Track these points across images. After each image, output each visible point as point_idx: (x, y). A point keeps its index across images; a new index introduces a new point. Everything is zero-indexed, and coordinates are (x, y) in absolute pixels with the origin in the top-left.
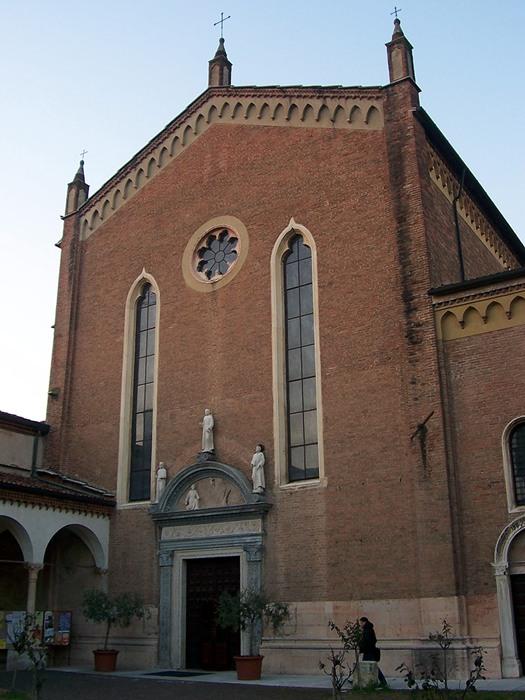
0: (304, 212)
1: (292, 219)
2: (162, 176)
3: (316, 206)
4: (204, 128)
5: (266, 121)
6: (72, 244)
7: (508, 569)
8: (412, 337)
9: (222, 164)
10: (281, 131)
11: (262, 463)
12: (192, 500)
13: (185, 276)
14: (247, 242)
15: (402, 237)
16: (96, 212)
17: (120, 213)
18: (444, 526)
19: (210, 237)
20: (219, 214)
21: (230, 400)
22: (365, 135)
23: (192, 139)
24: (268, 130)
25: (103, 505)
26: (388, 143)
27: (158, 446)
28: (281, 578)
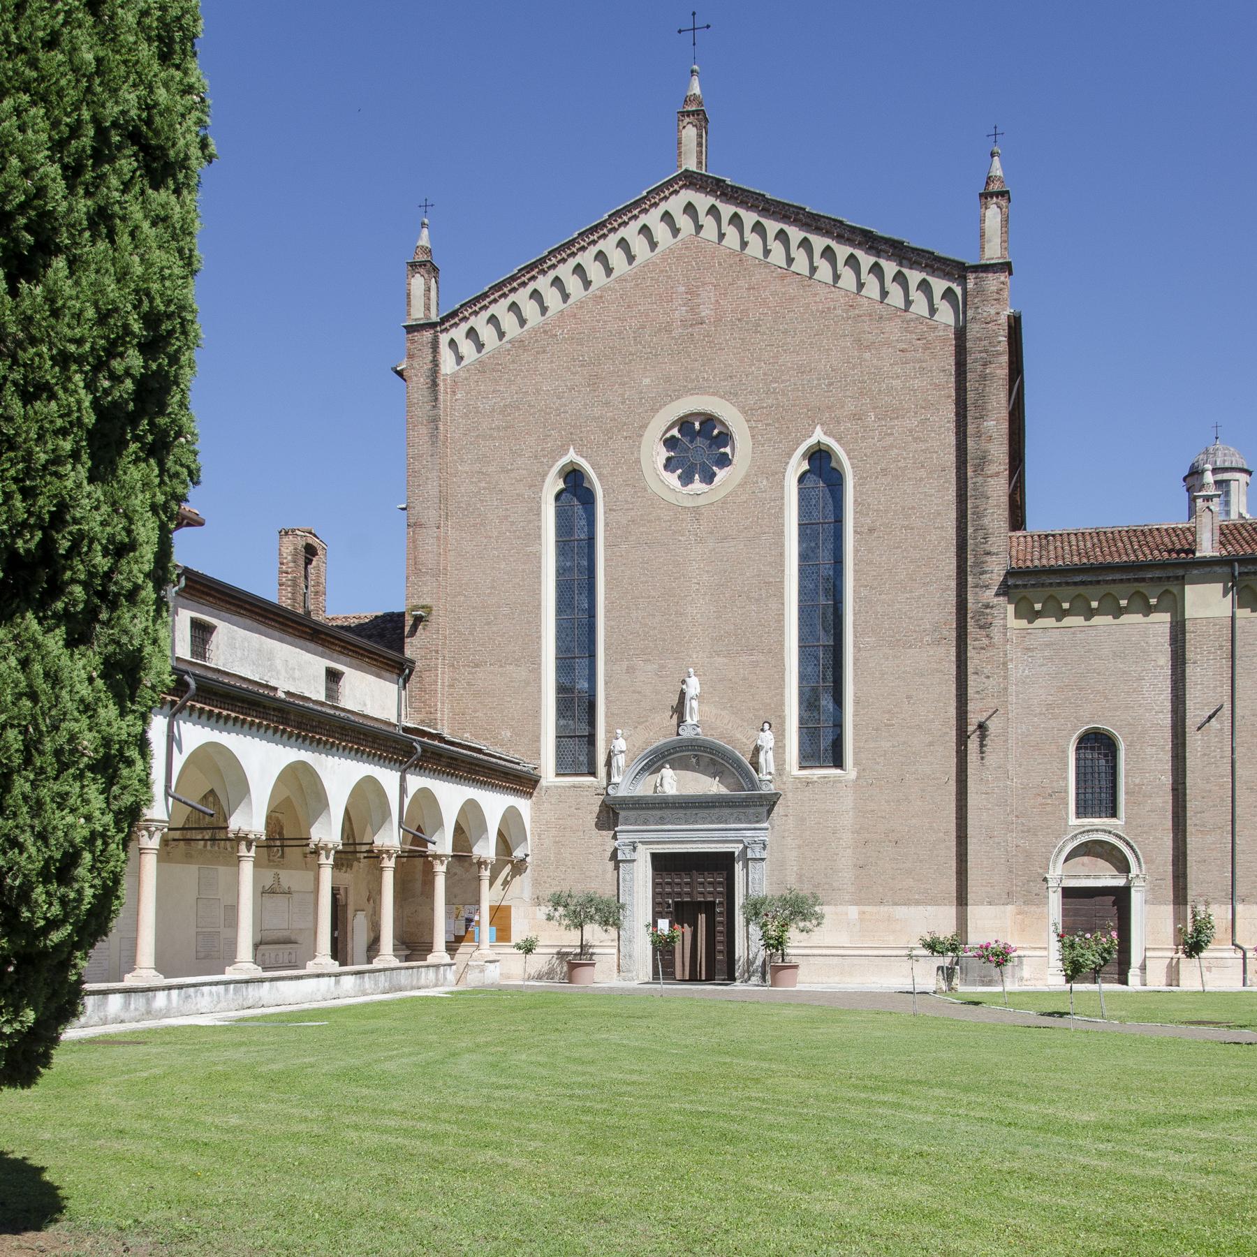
1: (818, 428)
3: (857, 417)
21: (720, 660)
27: (607, 708)
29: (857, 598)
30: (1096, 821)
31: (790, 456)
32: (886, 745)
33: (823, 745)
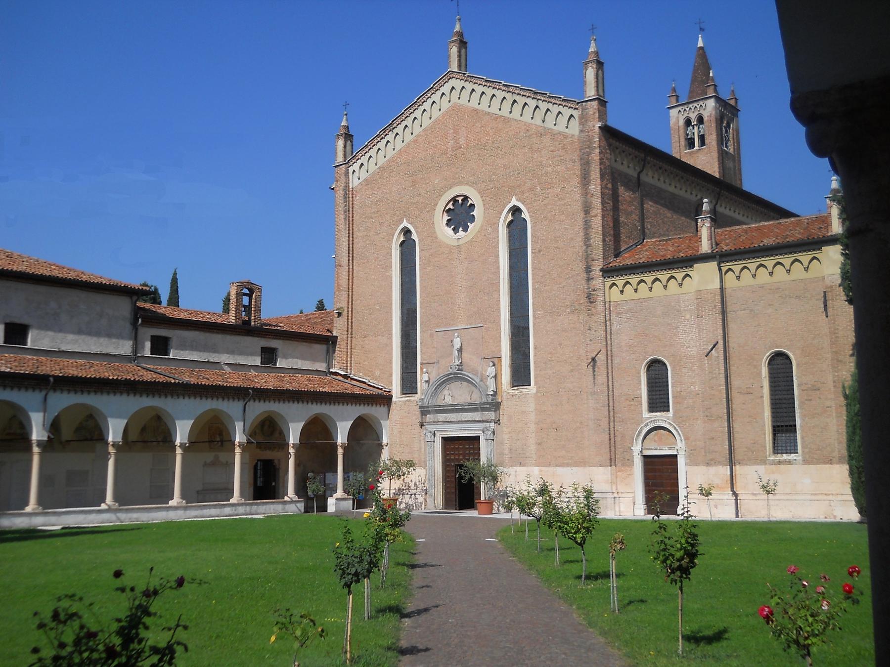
0: (523, 193)
2: (415, 141)
3: (532, 189)
4: (445, 105)
5: (494, 109)
6: (345, 190)
7: (641, 452)
8: (590, 298)
9: (462, 141)
10: (506, 120)
11: (493, 374)
12: (447, 397)
13: (437, 230)
14: (482, 208)
15: (587, 226)
16: (362, 164)
17: (382, 169)
18: (604, 423)
19: (454, 200)
20: (460, 183)
22: (566, 137)
23: (436, 114)
24: (497, 118)
25: (385, 400)
26: (581, 150)
28: (507, 452)
29: (534, 289)
30: (658, 414)
31: (501, 214)
32: (550, 372)
33: (521, 376)
